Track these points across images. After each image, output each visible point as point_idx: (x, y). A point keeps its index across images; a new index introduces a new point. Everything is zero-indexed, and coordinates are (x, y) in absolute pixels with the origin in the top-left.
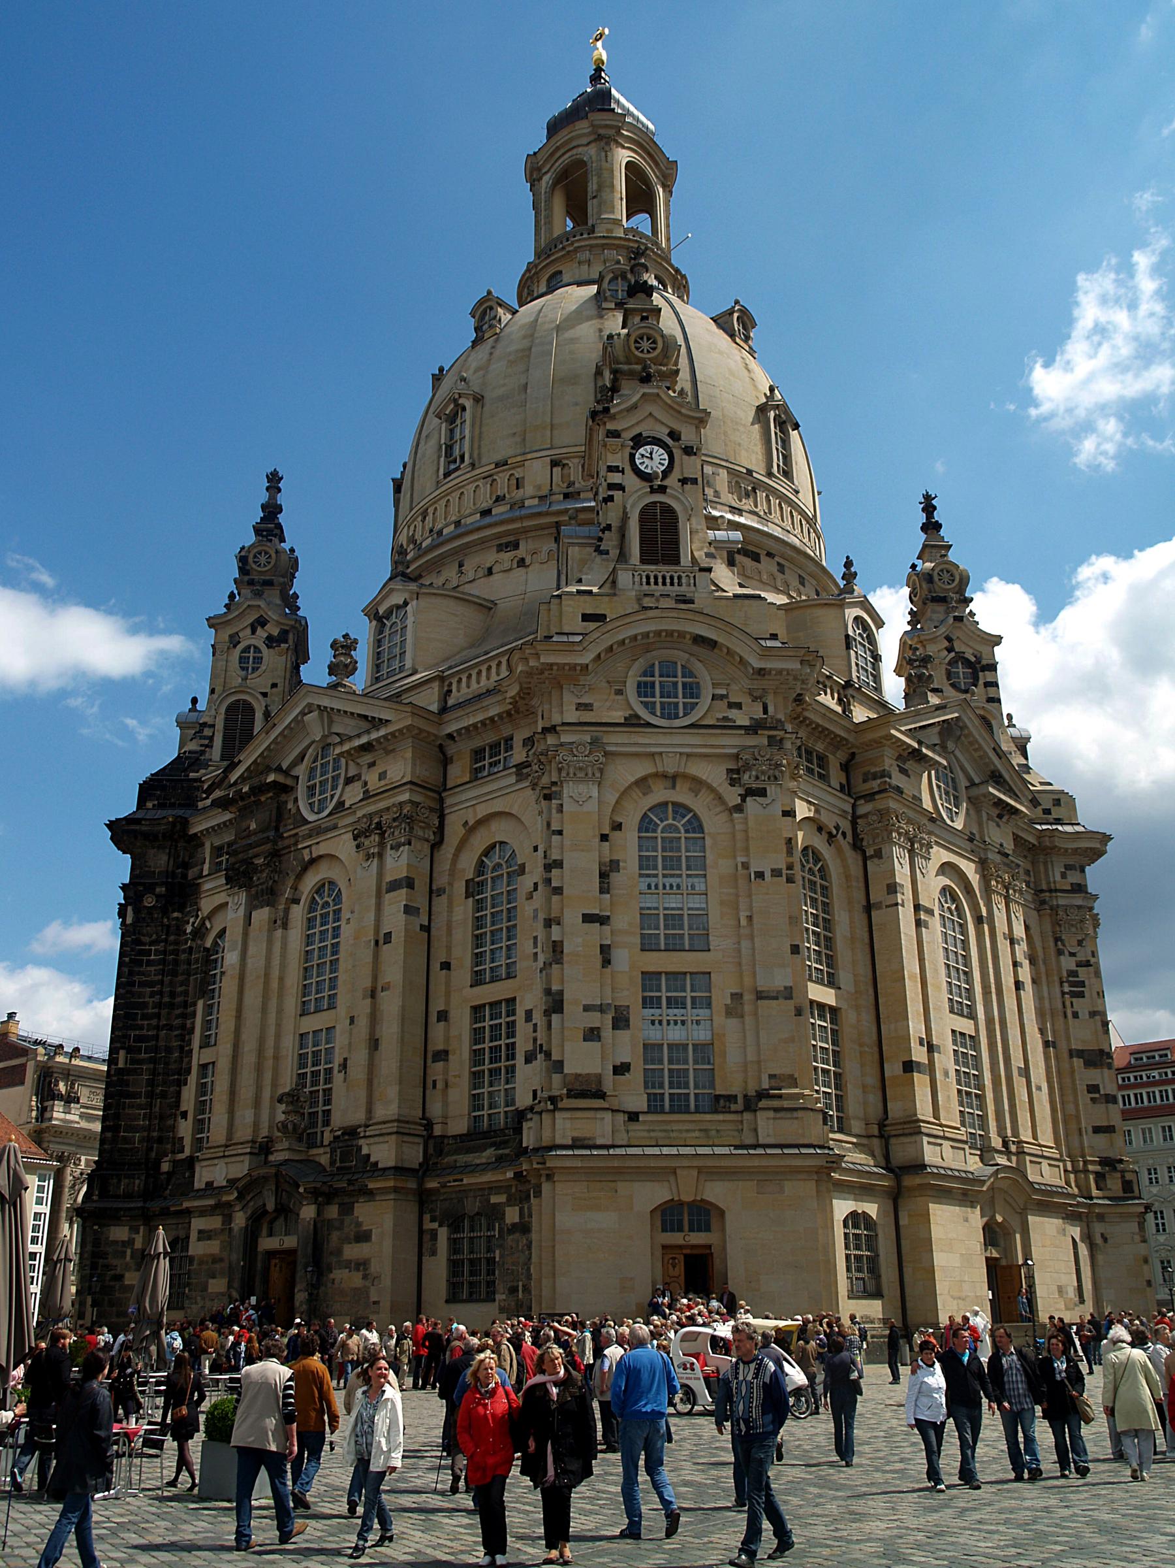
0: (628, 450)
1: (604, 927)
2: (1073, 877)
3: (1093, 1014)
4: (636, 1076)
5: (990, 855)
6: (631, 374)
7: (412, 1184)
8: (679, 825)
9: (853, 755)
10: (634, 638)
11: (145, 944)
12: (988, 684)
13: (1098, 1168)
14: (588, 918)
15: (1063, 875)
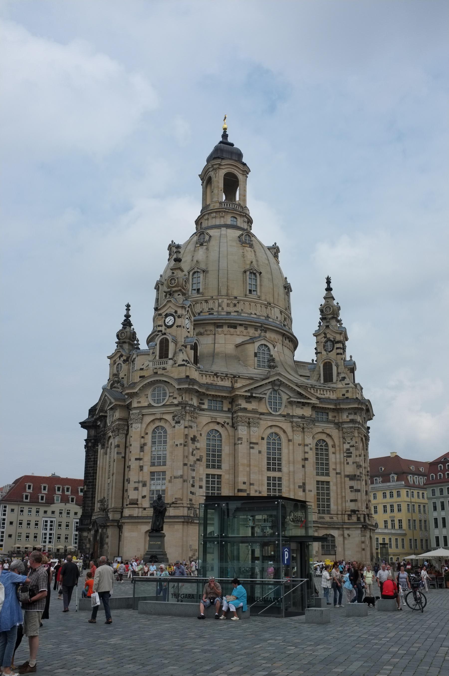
0: (164, 319)
1: (141, 462)
2: (351, 417)
3: (353, 463)
4: (147, 498)
5: (294, 420)
6: (168, 292)
7: (116, 524)
8: (162, 432)
9: (233, 399)
10: (148, 383)
11: (89, 456)
12: (337, 348)
13: (349, 513)
14: (136, 459)
15: (347, 417)
